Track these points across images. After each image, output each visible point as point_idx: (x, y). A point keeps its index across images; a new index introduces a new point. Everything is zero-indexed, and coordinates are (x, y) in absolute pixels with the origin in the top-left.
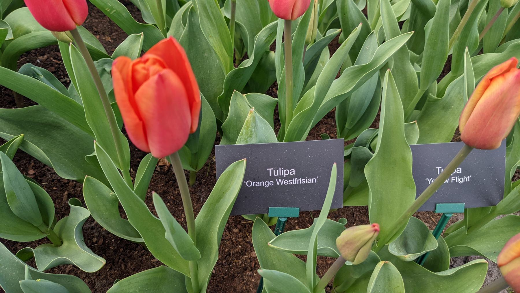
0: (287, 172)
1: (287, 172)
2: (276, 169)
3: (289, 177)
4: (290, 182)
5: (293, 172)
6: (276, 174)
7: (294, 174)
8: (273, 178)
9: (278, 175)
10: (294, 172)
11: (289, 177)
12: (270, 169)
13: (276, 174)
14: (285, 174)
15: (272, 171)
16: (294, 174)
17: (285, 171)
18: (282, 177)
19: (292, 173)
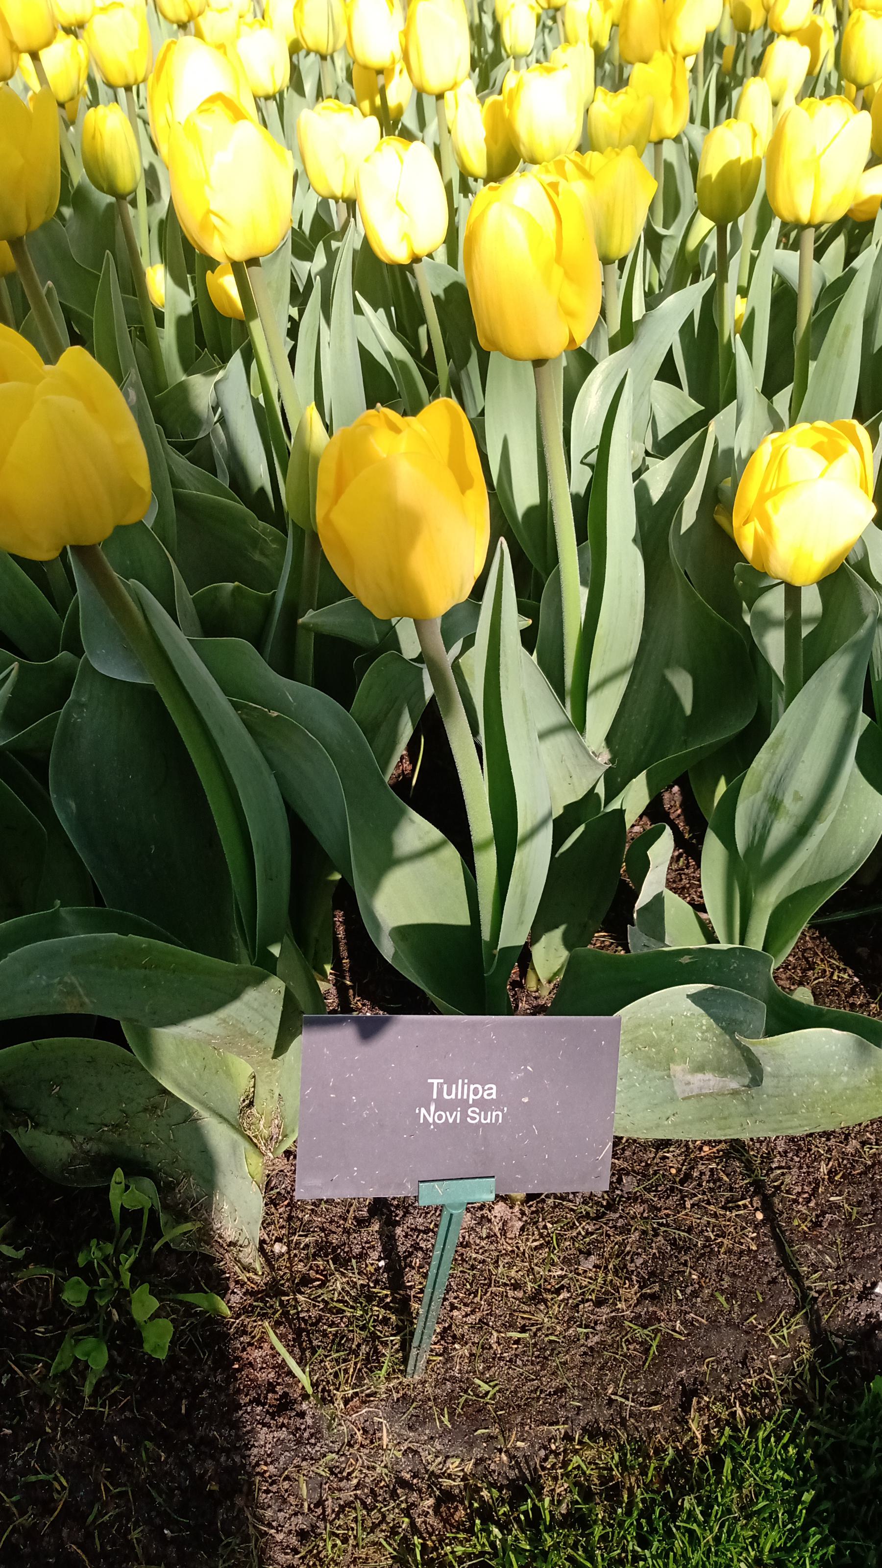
0: (476, 1092)
1: (476, 1092)
2: (450, 1081)
5: (491, 1092)
6: (449, 1094)
7: (494, 1096)
8: (443, 1105)
9: (453, 1096)
10: (494, 1091)
11: (484, 1105)
13: (449, 1094)
14: (472, 1096)
15: (440, 1086)
16: (494, 1096)
17: (472, 1087)
19: (489, 1095)
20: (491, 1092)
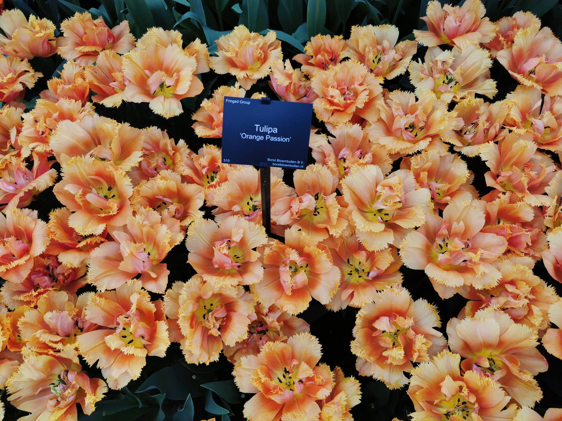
0: (270, 130)
1: (270, 130)
2: (262, 126)
4: (272, 139)
5: (275, 130)
6: (262, 130)
11: (272, 134)
12: (257, 126)
13: (262, 130)
15: (259, 127)
18: (266, 133)
20: (275, 130)
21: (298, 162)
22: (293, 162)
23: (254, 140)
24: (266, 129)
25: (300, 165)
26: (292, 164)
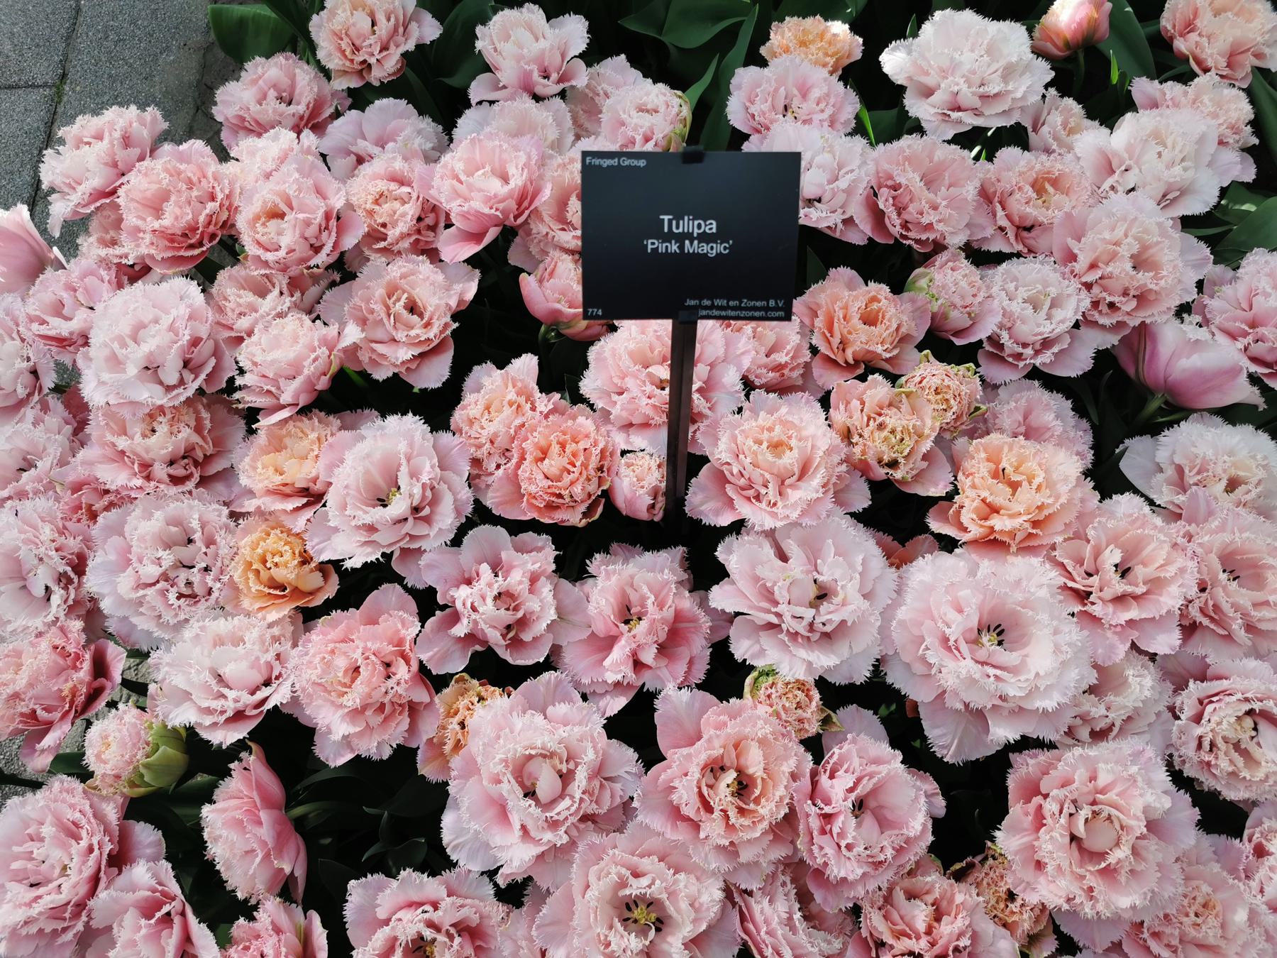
0: (699, 226)
1: (699, 226)
2: (679, 217)
3: (704, 238)
5: (712, 227)
6: (678, 227)
7: (714, 230)
10: (714, 226)
11: (704, 238)
12: (666, 218)
13: (678, 227)
14: (696, 231)
15: (670, 221)
16: (714, 230)
17: (696, 223)
18: (690, 236)
20: (712, 227)
21: (772, 303)
22: (758, 304)
23: (600, 166)
24: (688, 225)
25: (777, 309)
26: (755, 309)
